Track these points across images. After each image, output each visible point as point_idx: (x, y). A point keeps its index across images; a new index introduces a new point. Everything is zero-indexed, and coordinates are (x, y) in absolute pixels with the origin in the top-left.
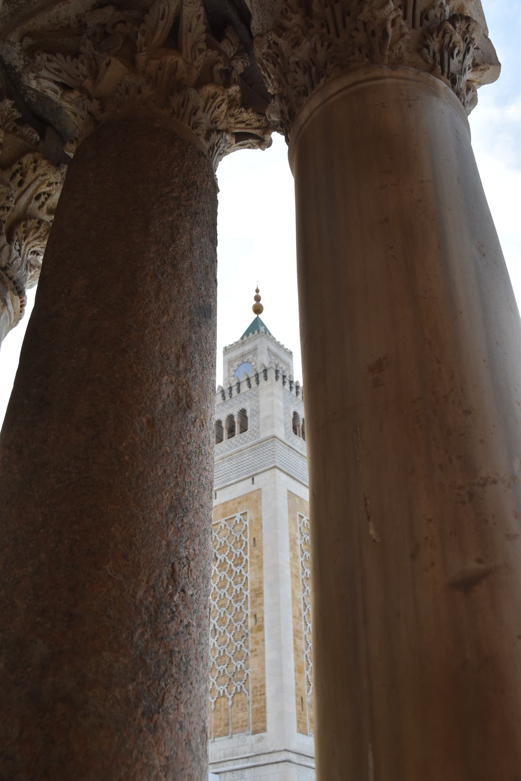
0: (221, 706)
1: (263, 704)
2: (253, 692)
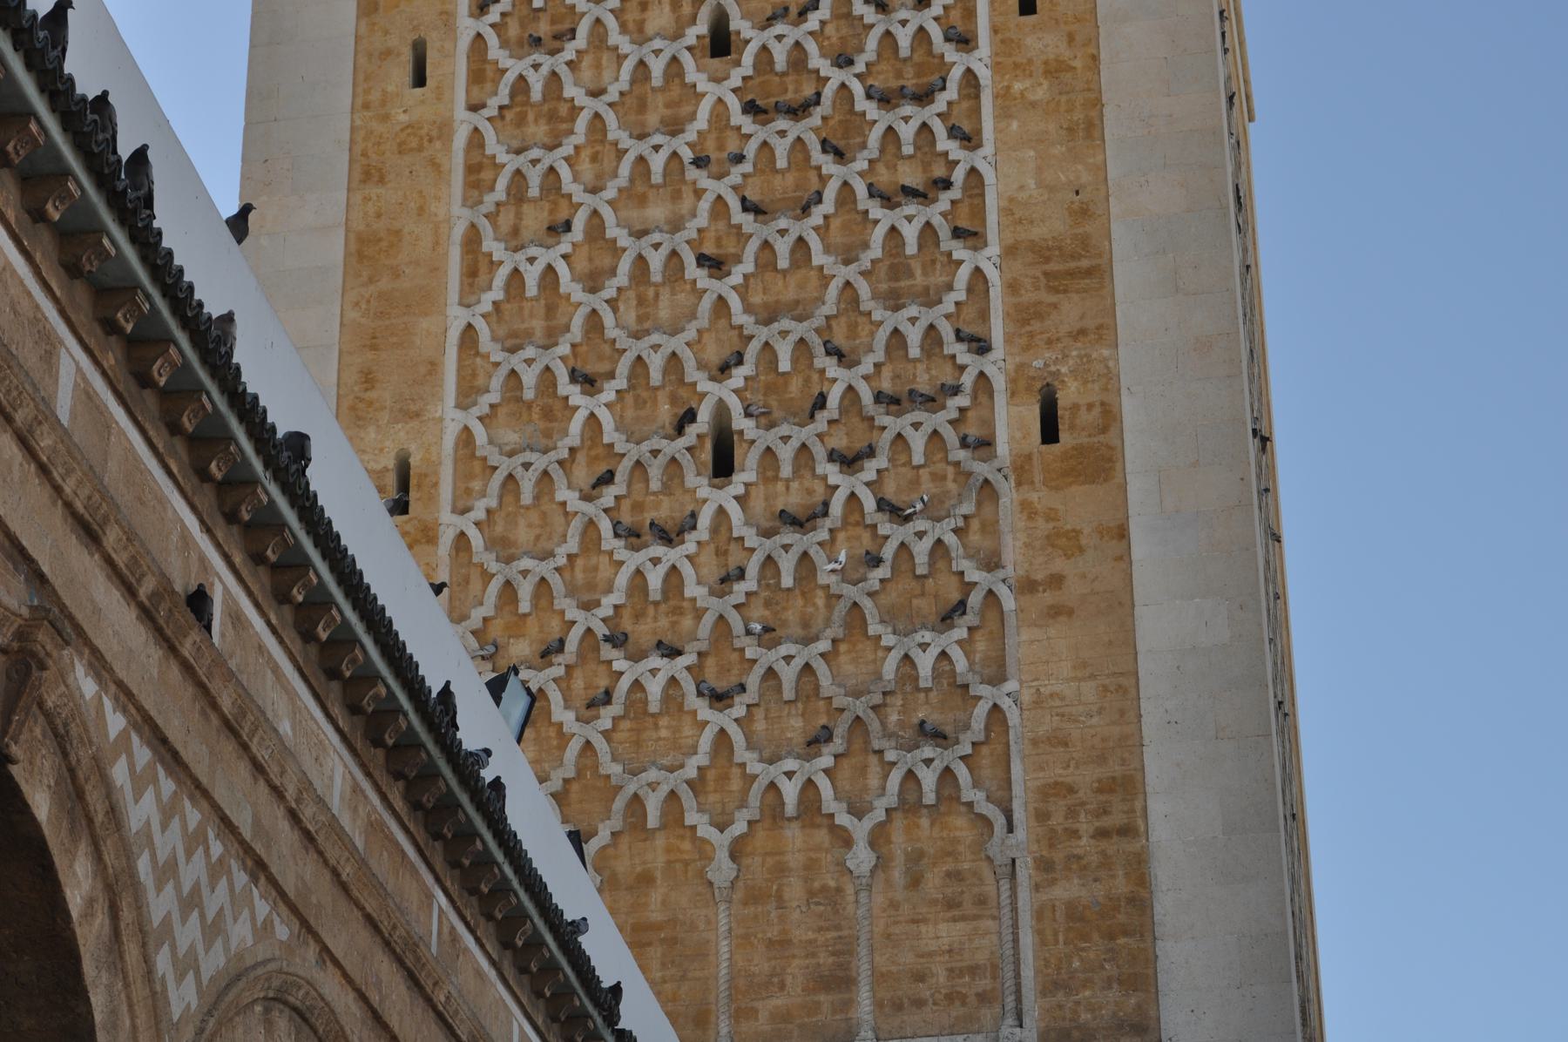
0: (781, 870)
1: (1121, 886)
2: (1042, 816)
